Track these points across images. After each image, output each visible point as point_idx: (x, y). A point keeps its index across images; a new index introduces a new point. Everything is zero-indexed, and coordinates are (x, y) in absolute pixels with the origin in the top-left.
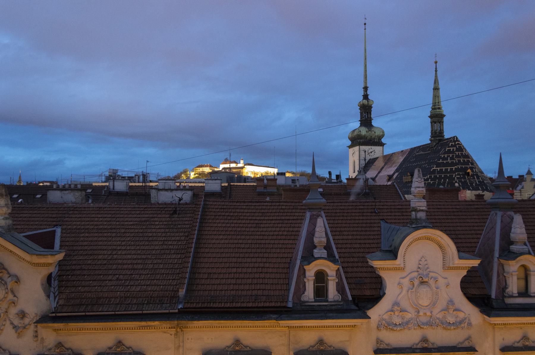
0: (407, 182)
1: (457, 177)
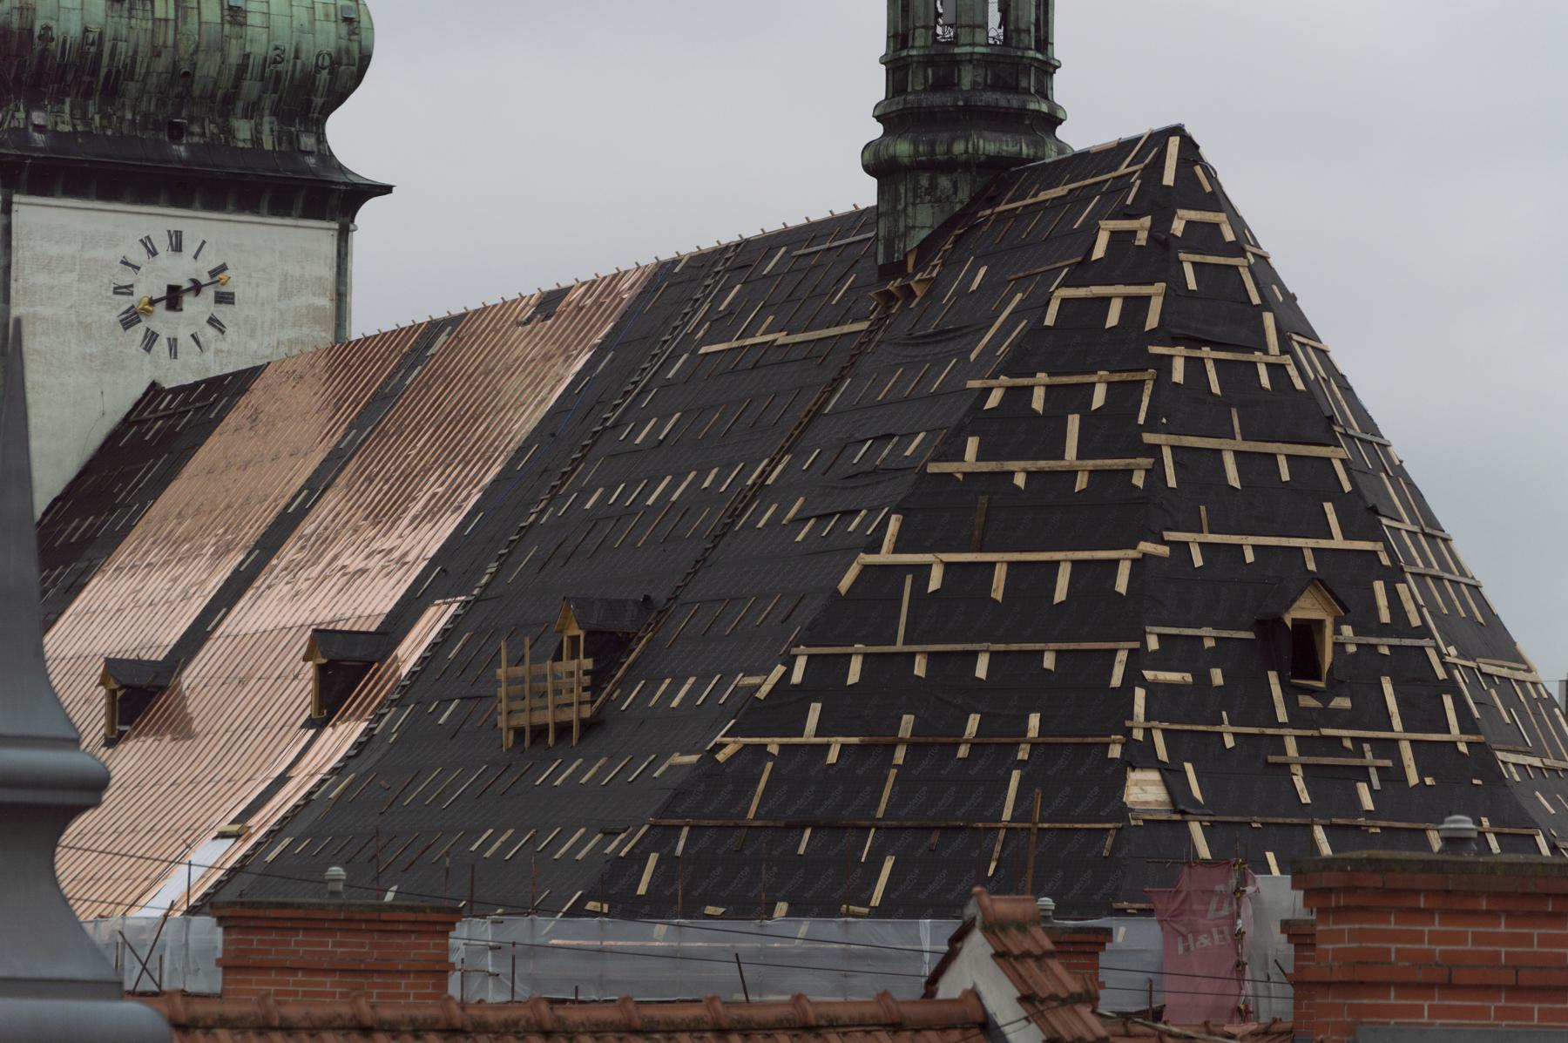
0: (539, 732)
1: (1152, 689)
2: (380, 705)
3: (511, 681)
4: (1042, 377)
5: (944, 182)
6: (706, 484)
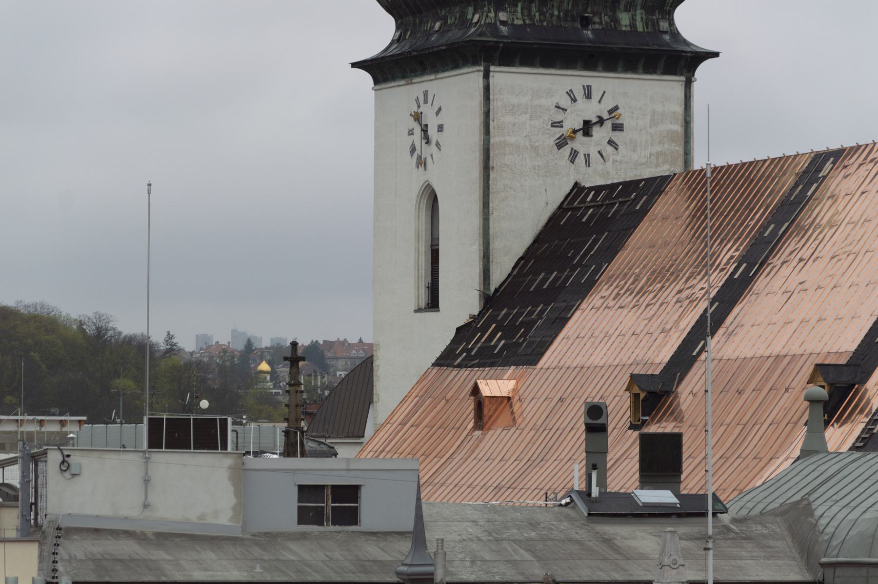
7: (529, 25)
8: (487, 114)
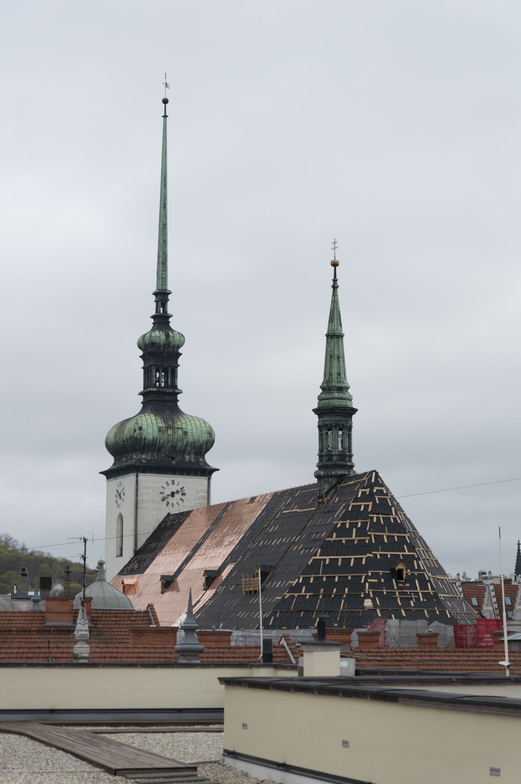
0: (251, 592)
1: (369, 583)
2: (219, 586)
3: (245, 582)
4: (348, 521)
5: (330, 479)
6: (283, 541)
7: (153, 460)
8: (137, 490)
